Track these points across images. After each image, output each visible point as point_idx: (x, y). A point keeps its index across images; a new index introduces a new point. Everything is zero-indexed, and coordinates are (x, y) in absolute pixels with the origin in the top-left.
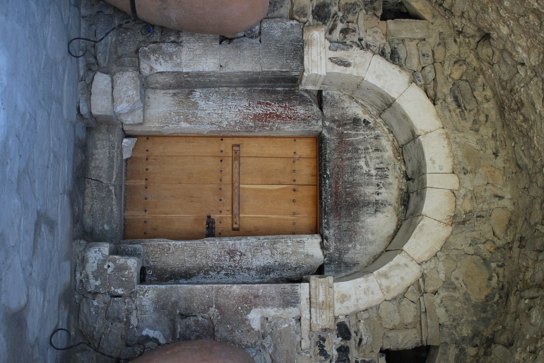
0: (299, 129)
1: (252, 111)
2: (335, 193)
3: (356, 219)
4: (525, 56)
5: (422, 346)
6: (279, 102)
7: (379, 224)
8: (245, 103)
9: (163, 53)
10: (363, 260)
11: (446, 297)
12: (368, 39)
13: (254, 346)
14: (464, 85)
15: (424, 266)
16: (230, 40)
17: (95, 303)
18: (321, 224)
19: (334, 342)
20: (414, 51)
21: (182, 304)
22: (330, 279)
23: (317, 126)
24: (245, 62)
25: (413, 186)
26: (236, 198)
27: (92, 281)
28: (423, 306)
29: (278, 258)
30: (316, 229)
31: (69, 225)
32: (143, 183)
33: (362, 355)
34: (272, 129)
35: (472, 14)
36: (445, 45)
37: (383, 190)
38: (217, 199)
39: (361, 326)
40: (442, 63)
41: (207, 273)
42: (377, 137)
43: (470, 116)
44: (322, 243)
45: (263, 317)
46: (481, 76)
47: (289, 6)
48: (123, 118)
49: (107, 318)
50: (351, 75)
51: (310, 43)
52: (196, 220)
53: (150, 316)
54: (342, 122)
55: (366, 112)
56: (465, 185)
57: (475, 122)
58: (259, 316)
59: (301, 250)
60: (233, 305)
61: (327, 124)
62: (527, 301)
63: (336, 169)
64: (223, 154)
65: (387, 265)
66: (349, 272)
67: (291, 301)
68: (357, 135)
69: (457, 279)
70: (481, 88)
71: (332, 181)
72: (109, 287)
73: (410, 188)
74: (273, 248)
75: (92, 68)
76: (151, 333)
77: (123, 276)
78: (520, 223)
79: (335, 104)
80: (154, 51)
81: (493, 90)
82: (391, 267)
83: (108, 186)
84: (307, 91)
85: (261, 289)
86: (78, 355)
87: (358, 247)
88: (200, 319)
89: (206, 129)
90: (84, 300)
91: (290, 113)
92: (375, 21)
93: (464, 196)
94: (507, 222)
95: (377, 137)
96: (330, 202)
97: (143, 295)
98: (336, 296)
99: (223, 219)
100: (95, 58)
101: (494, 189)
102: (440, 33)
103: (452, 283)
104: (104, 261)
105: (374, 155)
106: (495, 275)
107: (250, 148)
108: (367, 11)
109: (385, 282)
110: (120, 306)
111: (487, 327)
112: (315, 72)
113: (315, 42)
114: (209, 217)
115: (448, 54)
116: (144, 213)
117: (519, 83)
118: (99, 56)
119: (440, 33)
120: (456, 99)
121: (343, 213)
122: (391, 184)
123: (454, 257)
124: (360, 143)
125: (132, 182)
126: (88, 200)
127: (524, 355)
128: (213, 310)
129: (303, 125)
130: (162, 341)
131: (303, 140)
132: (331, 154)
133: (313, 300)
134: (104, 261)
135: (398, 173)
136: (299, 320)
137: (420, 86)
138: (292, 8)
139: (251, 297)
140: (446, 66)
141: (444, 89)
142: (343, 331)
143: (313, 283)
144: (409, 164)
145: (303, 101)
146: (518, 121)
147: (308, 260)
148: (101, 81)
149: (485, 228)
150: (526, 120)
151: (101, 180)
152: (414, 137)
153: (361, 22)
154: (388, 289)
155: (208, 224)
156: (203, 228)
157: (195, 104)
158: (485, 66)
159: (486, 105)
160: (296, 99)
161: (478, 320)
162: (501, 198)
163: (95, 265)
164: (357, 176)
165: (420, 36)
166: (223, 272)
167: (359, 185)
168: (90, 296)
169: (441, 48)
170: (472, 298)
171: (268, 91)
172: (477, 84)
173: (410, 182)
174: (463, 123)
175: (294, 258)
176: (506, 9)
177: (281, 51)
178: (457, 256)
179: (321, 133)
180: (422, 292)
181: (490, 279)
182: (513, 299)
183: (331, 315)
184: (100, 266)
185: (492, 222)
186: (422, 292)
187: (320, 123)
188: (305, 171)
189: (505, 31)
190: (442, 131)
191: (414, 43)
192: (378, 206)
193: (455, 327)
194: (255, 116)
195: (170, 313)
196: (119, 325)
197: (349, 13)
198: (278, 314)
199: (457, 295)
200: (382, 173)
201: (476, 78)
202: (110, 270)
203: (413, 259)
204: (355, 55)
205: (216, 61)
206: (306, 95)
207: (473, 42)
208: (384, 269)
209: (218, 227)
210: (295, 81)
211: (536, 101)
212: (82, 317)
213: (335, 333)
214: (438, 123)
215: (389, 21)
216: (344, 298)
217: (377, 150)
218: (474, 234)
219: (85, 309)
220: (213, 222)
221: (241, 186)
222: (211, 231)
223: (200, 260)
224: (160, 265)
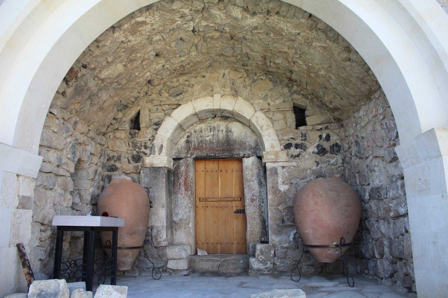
0: (191, 169)
1: (183, 192)
2: (222, 151)
3: (235, 141)
4: (160, 65)
5: (294, 110)
6: (179, 179)
7: (237, 131)
8: (179, 195)
9: (157, 235)
10: (254, 137)
11: (271, 100)
12: (149, 136)
13: (296, 188)
14: (171, 91)
15: (257, 109)
16: (151, 202)
17: (278, 264)
18: (237, 158)
19: (294, 151)
20: (155, 114)
21: (278, 222)
22: (264, 153)
23: (190, 160)
24: (161, 194)
25: (219, 114)
26: (226, 199)
27: (268, 266)
28: (275, 110)
29: (254, 178)
30: (240, 160)
31: (242, 277)
32: (219, 245)
33: (298, 138)
34: (192, 182)
35: (140, 88)
36: (152, 100)
37: (221, 129)
38: (226, 209)
39: (285, 138)
40: (161, 101)
41: (262, 212)
42: (195, 132)
43: (186, 88)
44: (247, 157)
45: (282, 184)
46: (167, 83)
47: (133, 174)
48: (188, 255)
49: (285, 258)
50: (167, 144)
51: (152, 164)
52: (237, 219)
53: (283, 237)
54: (188, 149)
55: (183, 137)
56: (219, 91)
57: (189, 86)
58: (282, 186)
59: (250, 167)
60: (277, 198)
61: (189, 155)
62: (272, 64)
63: (211, 151)
64: (204, 206)
65: (257, 126)
66: (260, 144)
67: (275, 171)
68: (194, 141)
69: (262, 94)
70: (173, 84)
71: (217, 153)
72: (271, 257)
73: (220, 116)
74: (250, 181)
75: (165, 269)
76: (292, 236)
77: (265, 251)
78: (236, 66)
79: (179, 152)
80: (156, 239)
81: (174, 78)
82: (258, 125)
83: (222, 262)
84: (174, 165)
85: (269, 185)
86: (303, 271)
87: (248, 140)
88: (284, 214)
89: (192, 214)
90: (277, 269)
91: (184, 173)
92: (141, 133)
93: (223, 91)
94: (236, 72)
96: (226, 154)
97: (274, 241)
98: (272, 150)
99: (236, 205)
100: (160, 268)
101: (220, 77)
102: (147, 102)
103: (264, 96)
104: (258, 260)
105: (204, 133)
106: (260, 77)
107: (201, 193)
108: (136, 137)
109: (265, 127)
110: (280, 252)
111: (284, 81)
112: (166, 162)
113: (151, 162)
114: (235, 212)
115: (157, 99)
116: (234, 244)
117: (172, 67)
118: (159, 266)
119: (147, 102)
120: (178, 95)
121: (232, 147)
122: (217, 125)
123: (252, 95)
124: (198, 140)
125: (219, 251)
126: (228, 271)
127: (296, 67)
128: (280, 208)
129: (190, 167)
130: (295, 231)
131: (197, 167)
132: (204, 154)
133: (274, 161)
134: (258, 260)
135: (212, 122)
136: (283, 167)
137: (172, 112)
138: (134, 173)
139: (274, 189)
140: (162, 100)
141: (173, 100)
142: (288, 146)
143: (266, 161)
144: (208, 116)
145: (178, 167)
146: (189, 67)
147: (255, 164)
148: (171, 265)
149: (239, 81)
150: (189, 64)
151: (218, 265)
152: (196, 114)
153: (141, 140)
154: (268, 126)
155: (238, 213)
156: (240, 215)
157: (180, 220)
158: (163, 82)
159: (181, 81)
160: (177, 171)
161: (281, 85)
162: (224, 74)
163: (260, 264)
164: (214, 141)
165: (147, 112)
166: (262, 204)
167: (218, 140)
168: (275, 267)
169: (154, 102)
170: (271, 87)
171: (173, 184)
172: (171, 85)
173: (217, 116)
174: (189, 92)
175: (254, 170)
176: (139, 74)
177: (156, 178)
178: (251, 94)
179: (193, 158)
180: (269, 110)
181: (262, 79)
182: (271, 70)
183: (281, 152)
184: (261, 262)
185: (235, 78)
186: (269, 110)
187: (189, 159)
188: (211, 166)
189: (148, 74)
190: (193, 101)
191: (151, 114)
192: (228, 131)
193: (284, 95)
194: (186, 190)
195: (282, 228)
196: (288, 252)
197: (137, 146)
198: (281, 177)
199: (270, 95)
200: (212, 129)
201: (168, 85)
202: (263, 258)
203: (254, 115)
204: (157, 142)
205: (161, 209)
206: (175, 166)
207: (151, 87)
208: (259, 128)
209: (240, 208)
210: (169, 171)
211: (181, 60)
212: (285, 270)
213: (289, 150)
214: (190, 103)
215: (141, 126)
216: (273, 146)
217: (201, 132)
218: (241, 86)
219: (281, 269)
220: (237, 210)
221: (219, 197)
222: (242, 211)
223: (256, 216)
224: (259, 235)
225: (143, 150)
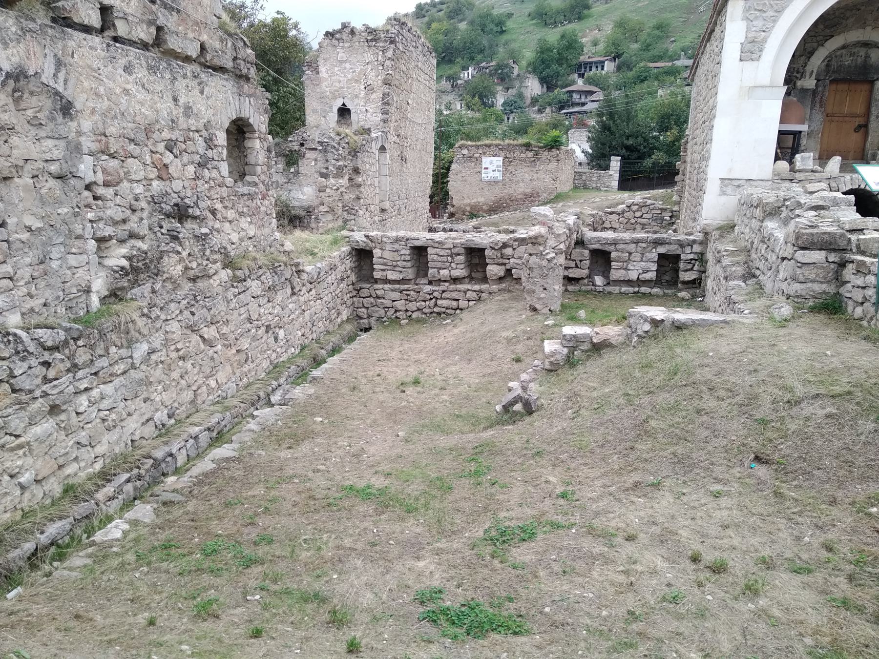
42: (836, 57)
95: (836, 57)
107: (829, 111)
192: (867, 56)
204: (808, 69)
209: (862, 123)
225: (795, 74)
